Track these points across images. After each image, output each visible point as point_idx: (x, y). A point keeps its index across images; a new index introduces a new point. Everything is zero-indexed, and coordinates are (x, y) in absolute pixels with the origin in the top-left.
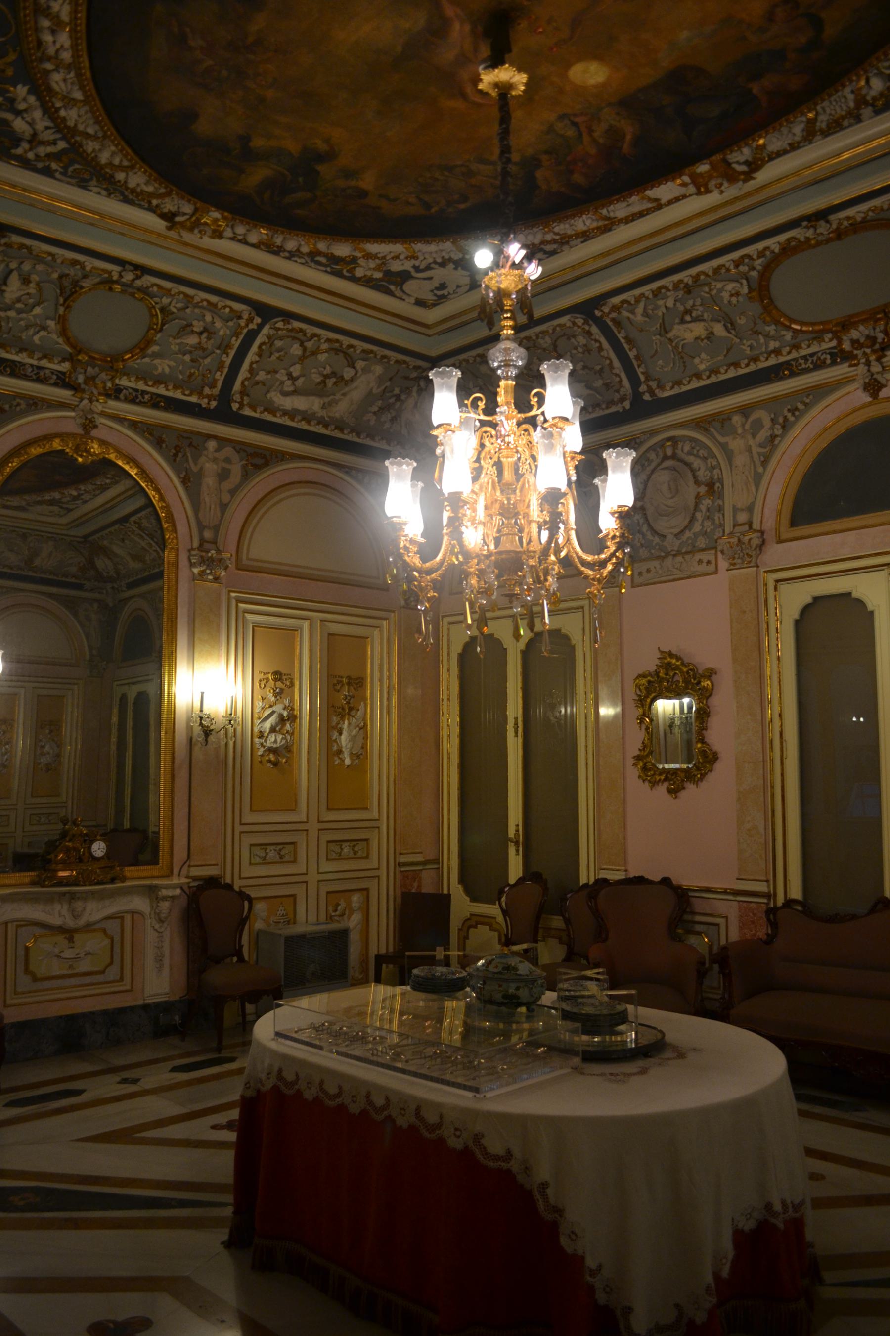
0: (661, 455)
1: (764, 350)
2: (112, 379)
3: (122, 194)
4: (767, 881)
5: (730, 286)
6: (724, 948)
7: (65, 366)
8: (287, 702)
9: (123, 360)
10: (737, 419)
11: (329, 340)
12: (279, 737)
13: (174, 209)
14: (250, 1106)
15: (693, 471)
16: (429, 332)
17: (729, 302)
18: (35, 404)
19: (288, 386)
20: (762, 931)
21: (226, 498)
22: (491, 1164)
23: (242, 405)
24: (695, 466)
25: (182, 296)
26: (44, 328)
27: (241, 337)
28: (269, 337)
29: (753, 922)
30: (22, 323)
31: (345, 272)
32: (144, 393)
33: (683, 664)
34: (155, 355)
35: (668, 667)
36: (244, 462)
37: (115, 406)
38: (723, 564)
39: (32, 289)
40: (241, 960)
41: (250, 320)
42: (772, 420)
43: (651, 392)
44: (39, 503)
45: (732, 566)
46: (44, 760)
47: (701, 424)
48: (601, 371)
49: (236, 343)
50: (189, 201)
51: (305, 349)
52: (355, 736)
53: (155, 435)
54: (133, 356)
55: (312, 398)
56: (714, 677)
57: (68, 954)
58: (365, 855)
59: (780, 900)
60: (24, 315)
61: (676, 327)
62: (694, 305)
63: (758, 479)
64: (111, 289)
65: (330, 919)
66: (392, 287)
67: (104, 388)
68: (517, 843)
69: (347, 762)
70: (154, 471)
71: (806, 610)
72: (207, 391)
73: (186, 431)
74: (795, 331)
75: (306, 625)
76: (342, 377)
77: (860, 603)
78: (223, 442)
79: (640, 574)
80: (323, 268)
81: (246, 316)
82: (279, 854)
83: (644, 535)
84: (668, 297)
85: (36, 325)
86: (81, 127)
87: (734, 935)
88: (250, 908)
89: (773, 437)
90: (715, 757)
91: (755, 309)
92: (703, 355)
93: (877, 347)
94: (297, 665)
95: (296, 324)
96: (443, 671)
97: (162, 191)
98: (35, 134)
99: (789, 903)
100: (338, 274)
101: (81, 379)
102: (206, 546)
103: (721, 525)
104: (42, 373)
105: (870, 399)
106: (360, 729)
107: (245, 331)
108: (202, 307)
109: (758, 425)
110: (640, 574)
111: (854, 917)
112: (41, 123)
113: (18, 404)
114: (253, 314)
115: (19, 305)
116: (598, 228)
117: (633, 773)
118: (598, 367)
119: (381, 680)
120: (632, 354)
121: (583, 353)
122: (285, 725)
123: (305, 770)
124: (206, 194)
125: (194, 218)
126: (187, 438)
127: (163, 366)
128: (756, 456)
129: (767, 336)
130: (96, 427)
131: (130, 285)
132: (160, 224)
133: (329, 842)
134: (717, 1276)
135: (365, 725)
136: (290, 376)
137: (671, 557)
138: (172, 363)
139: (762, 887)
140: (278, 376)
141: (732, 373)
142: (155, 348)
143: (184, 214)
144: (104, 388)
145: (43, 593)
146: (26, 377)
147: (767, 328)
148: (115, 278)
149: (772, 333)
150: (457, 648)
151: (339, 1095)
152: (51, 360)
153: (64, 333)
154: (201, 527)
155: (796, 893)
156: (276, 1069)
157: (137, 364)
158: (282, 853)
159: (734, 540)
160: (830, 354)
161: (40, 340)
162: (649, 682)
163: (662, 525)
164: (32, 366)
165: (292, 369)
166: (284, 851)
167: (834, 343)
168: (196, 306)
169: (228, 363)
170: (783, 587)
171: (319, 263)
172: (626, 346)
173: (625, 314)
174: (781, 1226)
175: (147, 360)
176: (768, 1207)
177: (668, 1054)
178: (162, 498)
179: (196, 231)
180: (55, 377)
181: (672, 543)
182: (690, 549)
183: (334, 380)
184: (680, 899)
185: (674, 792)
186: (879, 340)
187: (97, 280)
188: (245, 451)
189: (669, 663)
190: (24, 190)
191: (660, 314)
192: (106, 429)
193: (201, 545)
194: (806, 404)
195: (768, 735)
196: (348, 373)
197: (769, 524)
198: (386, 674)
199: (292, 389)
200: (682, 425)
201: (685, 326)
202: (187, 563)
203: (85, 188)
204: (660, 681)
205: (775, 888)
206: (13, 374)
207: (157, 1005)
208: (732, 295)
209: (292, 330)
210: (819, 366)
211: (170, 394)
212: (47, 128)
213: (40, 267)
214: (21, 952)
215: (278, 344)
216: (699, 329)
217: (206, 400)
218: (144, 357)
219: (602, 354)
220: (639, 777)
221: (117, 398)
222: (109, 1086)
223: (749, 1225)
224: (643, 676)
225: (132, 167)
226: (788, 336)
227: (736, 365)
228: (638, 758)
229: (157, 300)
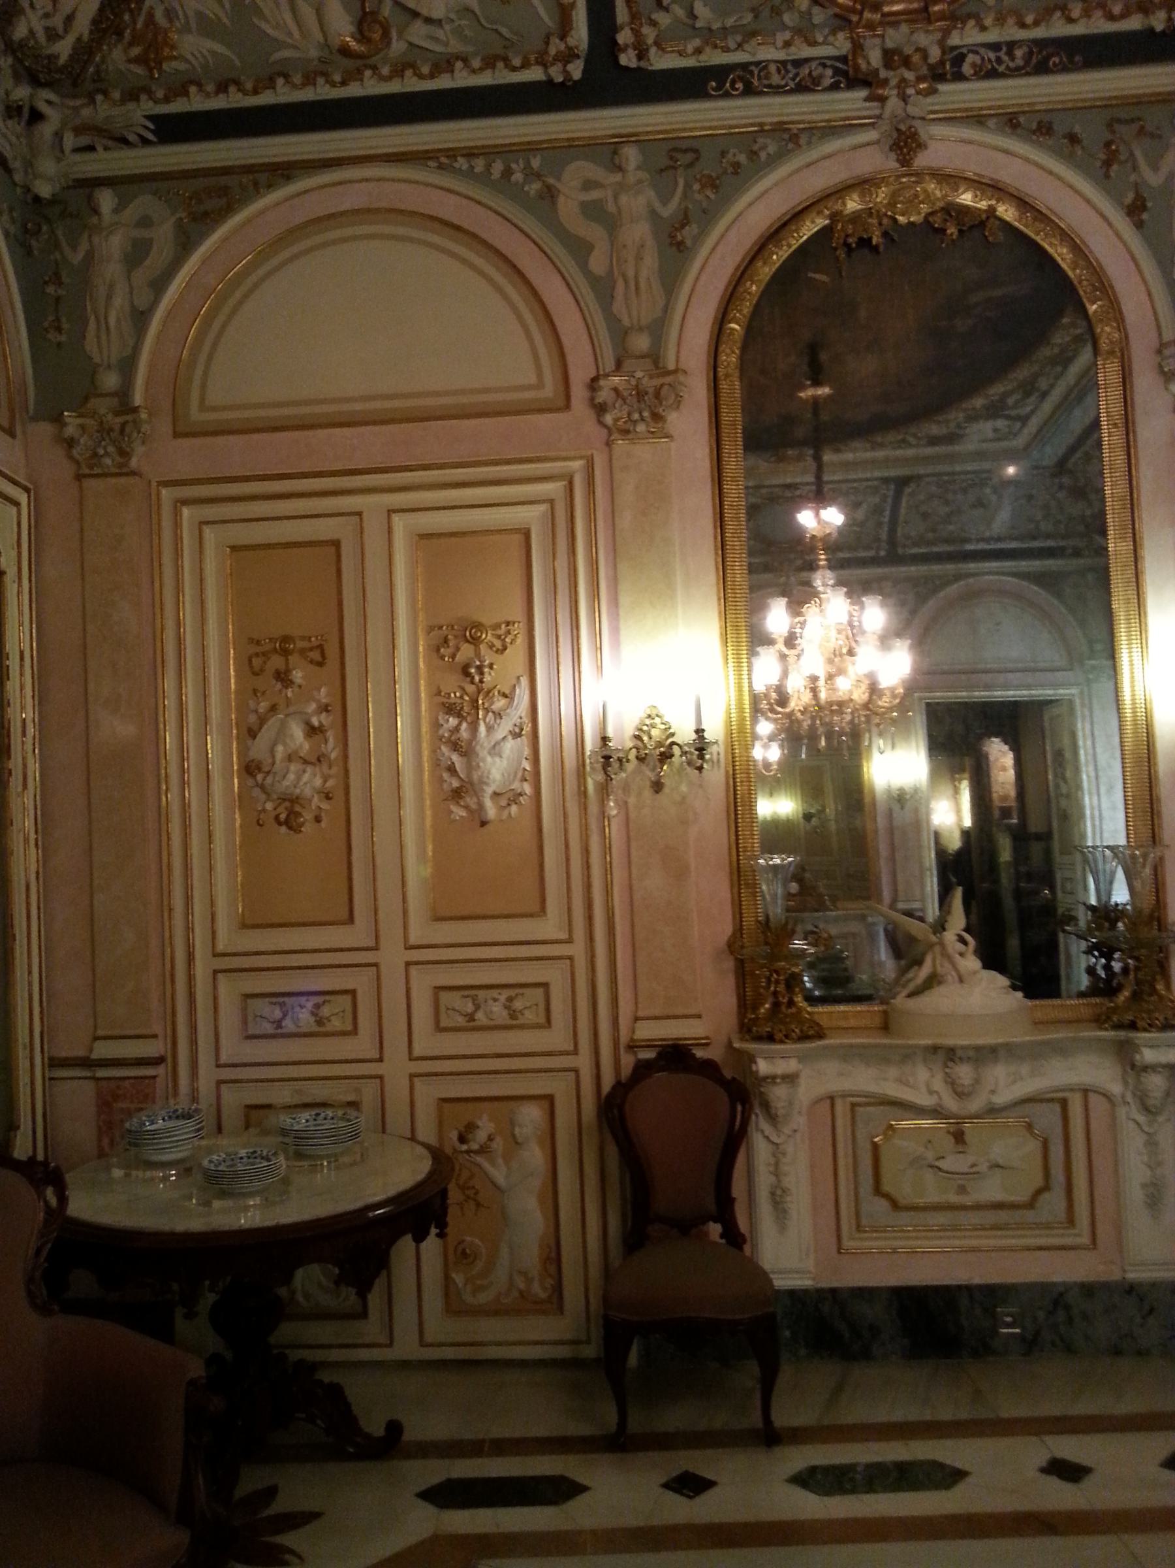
37: (953, 94)
101: (875, 57)
113: (764, 148)
126: (1133, 120)
180: (829, 72)
192: (945, 147)
211: (1078, 29)
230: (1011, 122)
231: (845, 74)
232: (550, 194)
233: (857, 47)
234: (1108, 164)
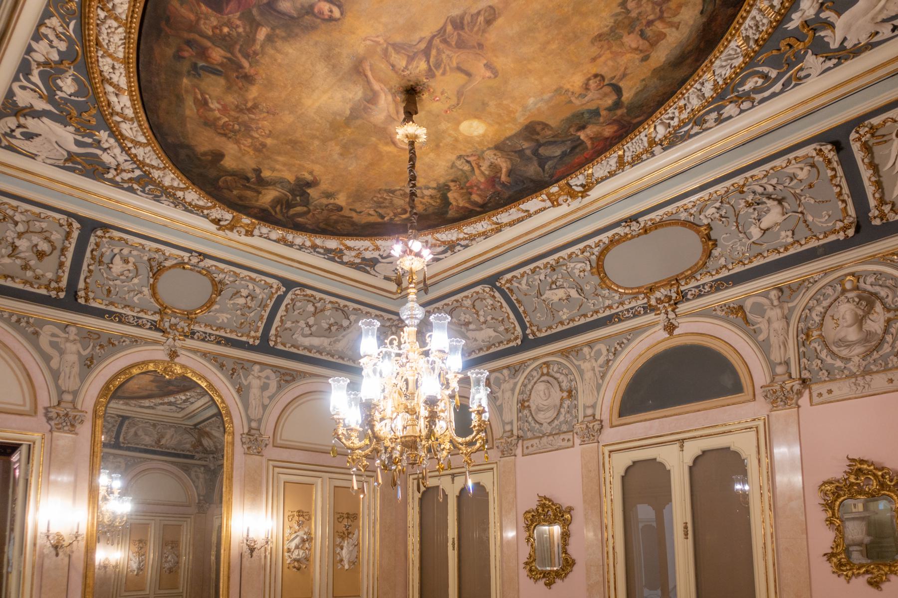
0: (540, 373)
2: (189, 325)
3: (184, 206)
7: (157, 318)
11: (331, 302)
13: (219, 217)
16: (394, 297)
18: (136, 341)
19: (307, 331)
23: (276, 342)
24: (560, 380)
28: (292, 300)
30: (126, 289)
37: (189, 343)
39: (130, 266)
47: (565, 353)
49: (271, 304)
51: (316, 308)
55: (322, 339)
64: (184, 268)
69: (347, 567)
72: (252, 333)
73: (239, 359)
74: (621, 293)
76: (342, 326)
83: (530, 424)
85: (134, 290)
86: (148, 161)
91: (596, 280)
92: (565, 310)
93: (672, 302)
95: (309, 292)
97: (210, 204)
98: (118, 165)
101: (167, 325)
112: (122, 158)
115: (122, 277)
123: (319, 571)
124: (239, 206)
127: (223, 318)
128: (597, 373)
129: (603, 297)
130: (178, 356)
132: (213, 227)
136: (307, 325)
138: (229, 316)
142: (216, 307)
148: (186, 261)
149: (607, 295)
153: (154, 294)
167: (645, 301)
179: (235, 231)
183: (336, 327)
186: (674, 298)
187: (175, 262)
190: (117, 202)
194: (628, 340)
196: (345, 323)
203: (158, 201)
209: (306, 296)
210: (636, 315)
211: (228, 335)
212: (126, 161)
213: (135, 253)
215: (298, 304)
216: (561, 293)
221: (192, 338)
225: (187, 188)
226: (617, 297)
227: (585, 316)
230: (205, 355)
231: (155, 326)
232: (36, 333)
233: (162, 320)
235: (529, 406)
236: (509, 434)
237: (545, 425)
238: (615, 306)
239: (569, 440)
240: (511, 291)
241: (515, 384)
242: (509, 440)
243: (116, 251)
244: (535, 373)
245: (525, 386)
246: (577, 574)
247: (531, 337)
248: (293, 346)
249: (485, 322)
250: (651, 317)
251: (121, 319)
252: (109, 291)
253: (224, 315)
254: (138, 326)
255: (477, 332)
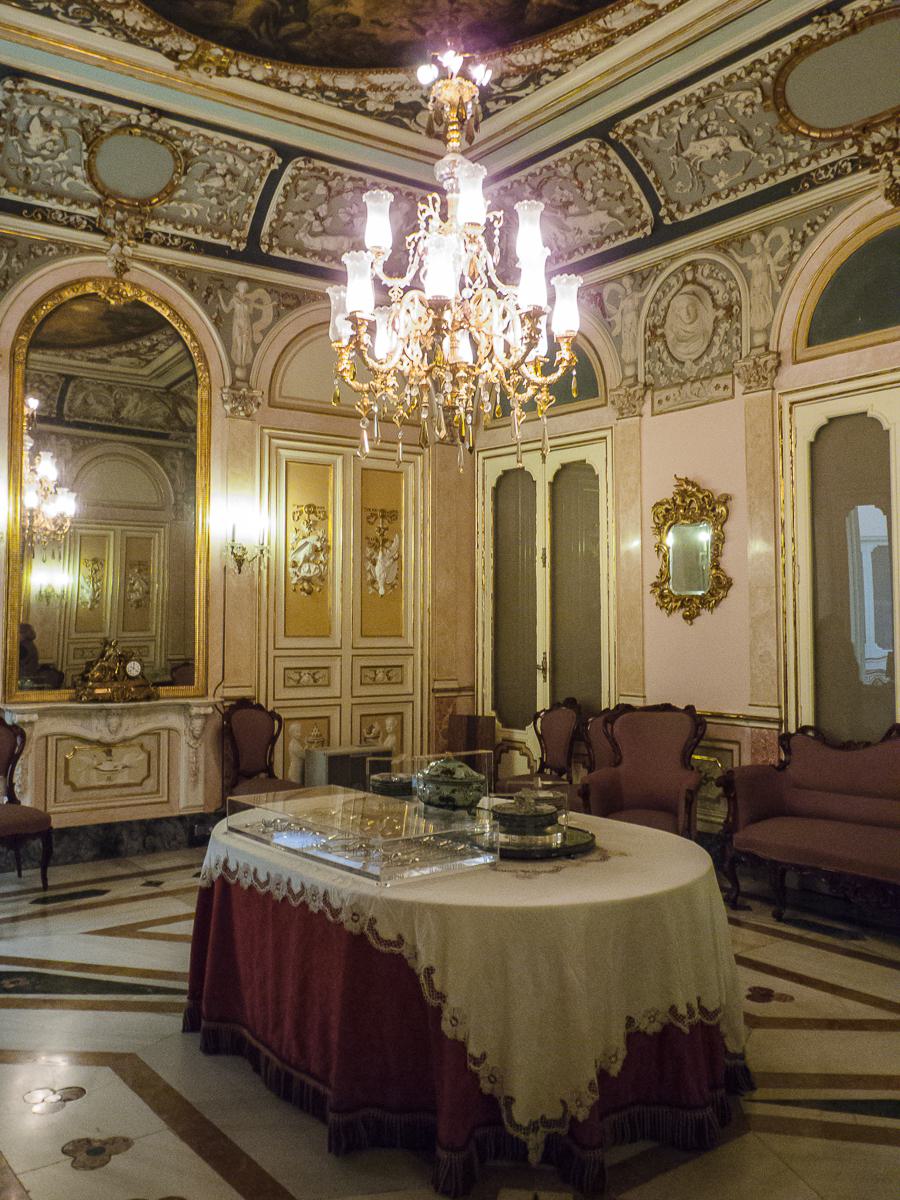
1: (782, 162)
2: (142, 223)
4: (779, 707)
5: (743, 96)
6: (731, 772)
7: (95, 212)
8: (320, 534)
9: (151, 205)
10: (756, 238)
11: (352, 179)
12: (313, 567)
14: (205, 895)
15: (711, 294)
17: (744, 113)
18: (67, 249)
19: (317, 227)
20: (775, 757)
21: (258, 338)
22: (383, 948)
23: (271, 247)
24: (714, 289)
25: (201, 138)
26: (72, 174)
27: (265, 179)
28: (293, 178)
29: (765, 748)
31: (356, 106)
32: (173, 236)
33: (699, 490)
34: (181, 199)
35: (683, 494)
36: (275, 303)
38: (739, 388)
40: (271, 775)
41: (271, 160)
42: (791, 236)
43: (671, 216)
44: (119, 354)
45: (748, 390)
46: (133, 597)
47: (722, 246)
48: (622, 197)
49: (260, 184)
50: (189, 38)
51: (329, 189)
52: (389, 567)
53: (186, 277)
54: (160, 201)
56: (729, 503)
57: (107, 766)
58: (399, 680)
59: (792, 729)
60: (49, 162)
61: (692, 144)
62: (708, 120)
63: (776, 298)
65: (363, 740)
66: (406, 120)
67: (133, 232)
68: (544, 670)
70: (186, 313)
71: (820, 431)
72: (235, 233)
73: (216, 273)
74: (814, 139)
75: (339, 459)
77: (875, 422)
78: (253, 283)
79: (660, 402)
80: (335, 104)
81: (266, 157)
82: (313, 677)
84: (681, 114)
87: (747, 761)
88: (280, 727)
89: (792, 255)
90: (729, 584)
91: (770, 119)
92: (722, 173)
94: (330, 498)
95: (319, 164)
96: (479, 508)
99: (803, 730)
100: (350, 109)
102: (238, 384)
103: (739, 349)
104: (72, 219)
105: (892, 207)
106: (394, 560)
107: (268, 172)
108: (222, 149)
109: (777, 243)
110: (660, 402)
111: (868, 744)
113: (51, 250)
114: (274, 154)
116: (599, 43)
117: (651, 600)
118: (619, 193)
119: (415, 514)
120: (651, 177)
121: (604, 180)
122: (319, 555)
125: (196, 56)
127: (189, 210)
129: (785, 147)
130: (127, 270)
131: (149, 129)
133: (362, 667)
134: (603, 1075)
135: (400, 556)
136: (317, 216)
137: (689, 384)
138: (200, 207)
139: (774, 714)
140: (305, 216)
141: (751, 190)
143: (187, 52)
144: (133, 232)
145: (132, 443)
146: (57, 223)
147: (785, 139)
149: (791, 143)
150: (491, 482)
151: (267, 883)
152: (80, 206)
154: (233, 366)
155: (807, 719)
156: (222, 860)
157: (166, 208)
158: (317, 677)
159: (750, 363)
160: (851, 161)
161: (68, 185)
162: (667, 510)
163: (681, 351)
164: (63, 212)
165: (318, 210)
166: (318, 675)
167: (855, 149)
168: (216, 148)
169: (255, 205)
170: (797, 409)
171: (329, 98)
172: (644, 169)
173: (641, 134)
174: (686, 1030)
175: (173, 204)
176: (673, 1010)
177: (594, 856)
178: (194, 338)
180: (85, 222)
181: (690, 369)
182: (708, 374)
184: (697, 725)
185: (689, 618)
188: (276, 292)
189: (685, 491)
191: (675, 131)
192: (138, 272)
193: (233, 383)
194: (825, 218)
195: (782, 560)
197: (786, 345)
198: (421, 507)
199: (320, 229)
200: (703, 248)
201: (701, 142)
202: (220, 401)
204: (677, 507)
205: (786, 713)
206: (45, 220)
207: (193, 817)
208: (746, 106)
209: (314, 169)
211: (199, 237)
214: (61, 764)
215: (302, 184)
217: (235, 243)
218: (170, 201)
219: (621, 179)
220: (657, 604)
221: (148, 242)
222: (136, 887)
223: (654, 1028)
224: (660, 504)
226: (807, 145)
227: (754, 181)
228: (655, 585)
229: (177, 143)
230: (166, 269)
231: (94, 226)
234: (207, 296)
235: (663, 336)
236: (631, 381)
237: (688, 364)
238: (803, 162)
239: (726, 387)
240: (634, 145)
241: (642, 301)
242: (632, 390)
243: (34, 111)
244: (673, 281)
245: (658, 303)
246: (735, 599)
247: (667, 221)
248: (296, 251)
249: (594, 201)
250: (864, 177)
251: (46, 216)
252: (27, 174)
253: (194, 204)
254: (70, 226)
255: (582, 219)
